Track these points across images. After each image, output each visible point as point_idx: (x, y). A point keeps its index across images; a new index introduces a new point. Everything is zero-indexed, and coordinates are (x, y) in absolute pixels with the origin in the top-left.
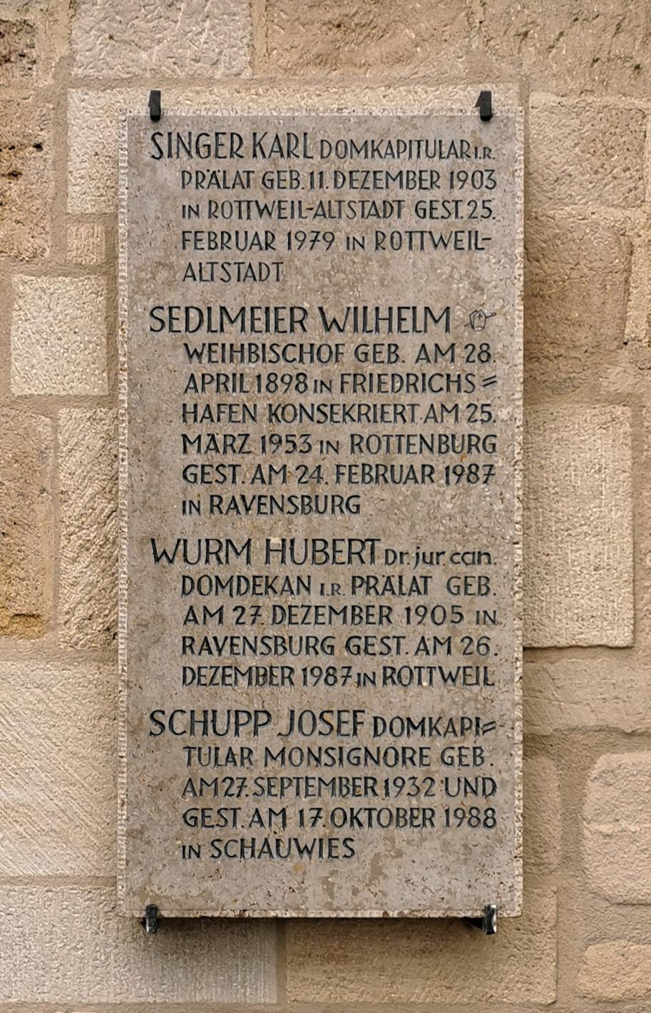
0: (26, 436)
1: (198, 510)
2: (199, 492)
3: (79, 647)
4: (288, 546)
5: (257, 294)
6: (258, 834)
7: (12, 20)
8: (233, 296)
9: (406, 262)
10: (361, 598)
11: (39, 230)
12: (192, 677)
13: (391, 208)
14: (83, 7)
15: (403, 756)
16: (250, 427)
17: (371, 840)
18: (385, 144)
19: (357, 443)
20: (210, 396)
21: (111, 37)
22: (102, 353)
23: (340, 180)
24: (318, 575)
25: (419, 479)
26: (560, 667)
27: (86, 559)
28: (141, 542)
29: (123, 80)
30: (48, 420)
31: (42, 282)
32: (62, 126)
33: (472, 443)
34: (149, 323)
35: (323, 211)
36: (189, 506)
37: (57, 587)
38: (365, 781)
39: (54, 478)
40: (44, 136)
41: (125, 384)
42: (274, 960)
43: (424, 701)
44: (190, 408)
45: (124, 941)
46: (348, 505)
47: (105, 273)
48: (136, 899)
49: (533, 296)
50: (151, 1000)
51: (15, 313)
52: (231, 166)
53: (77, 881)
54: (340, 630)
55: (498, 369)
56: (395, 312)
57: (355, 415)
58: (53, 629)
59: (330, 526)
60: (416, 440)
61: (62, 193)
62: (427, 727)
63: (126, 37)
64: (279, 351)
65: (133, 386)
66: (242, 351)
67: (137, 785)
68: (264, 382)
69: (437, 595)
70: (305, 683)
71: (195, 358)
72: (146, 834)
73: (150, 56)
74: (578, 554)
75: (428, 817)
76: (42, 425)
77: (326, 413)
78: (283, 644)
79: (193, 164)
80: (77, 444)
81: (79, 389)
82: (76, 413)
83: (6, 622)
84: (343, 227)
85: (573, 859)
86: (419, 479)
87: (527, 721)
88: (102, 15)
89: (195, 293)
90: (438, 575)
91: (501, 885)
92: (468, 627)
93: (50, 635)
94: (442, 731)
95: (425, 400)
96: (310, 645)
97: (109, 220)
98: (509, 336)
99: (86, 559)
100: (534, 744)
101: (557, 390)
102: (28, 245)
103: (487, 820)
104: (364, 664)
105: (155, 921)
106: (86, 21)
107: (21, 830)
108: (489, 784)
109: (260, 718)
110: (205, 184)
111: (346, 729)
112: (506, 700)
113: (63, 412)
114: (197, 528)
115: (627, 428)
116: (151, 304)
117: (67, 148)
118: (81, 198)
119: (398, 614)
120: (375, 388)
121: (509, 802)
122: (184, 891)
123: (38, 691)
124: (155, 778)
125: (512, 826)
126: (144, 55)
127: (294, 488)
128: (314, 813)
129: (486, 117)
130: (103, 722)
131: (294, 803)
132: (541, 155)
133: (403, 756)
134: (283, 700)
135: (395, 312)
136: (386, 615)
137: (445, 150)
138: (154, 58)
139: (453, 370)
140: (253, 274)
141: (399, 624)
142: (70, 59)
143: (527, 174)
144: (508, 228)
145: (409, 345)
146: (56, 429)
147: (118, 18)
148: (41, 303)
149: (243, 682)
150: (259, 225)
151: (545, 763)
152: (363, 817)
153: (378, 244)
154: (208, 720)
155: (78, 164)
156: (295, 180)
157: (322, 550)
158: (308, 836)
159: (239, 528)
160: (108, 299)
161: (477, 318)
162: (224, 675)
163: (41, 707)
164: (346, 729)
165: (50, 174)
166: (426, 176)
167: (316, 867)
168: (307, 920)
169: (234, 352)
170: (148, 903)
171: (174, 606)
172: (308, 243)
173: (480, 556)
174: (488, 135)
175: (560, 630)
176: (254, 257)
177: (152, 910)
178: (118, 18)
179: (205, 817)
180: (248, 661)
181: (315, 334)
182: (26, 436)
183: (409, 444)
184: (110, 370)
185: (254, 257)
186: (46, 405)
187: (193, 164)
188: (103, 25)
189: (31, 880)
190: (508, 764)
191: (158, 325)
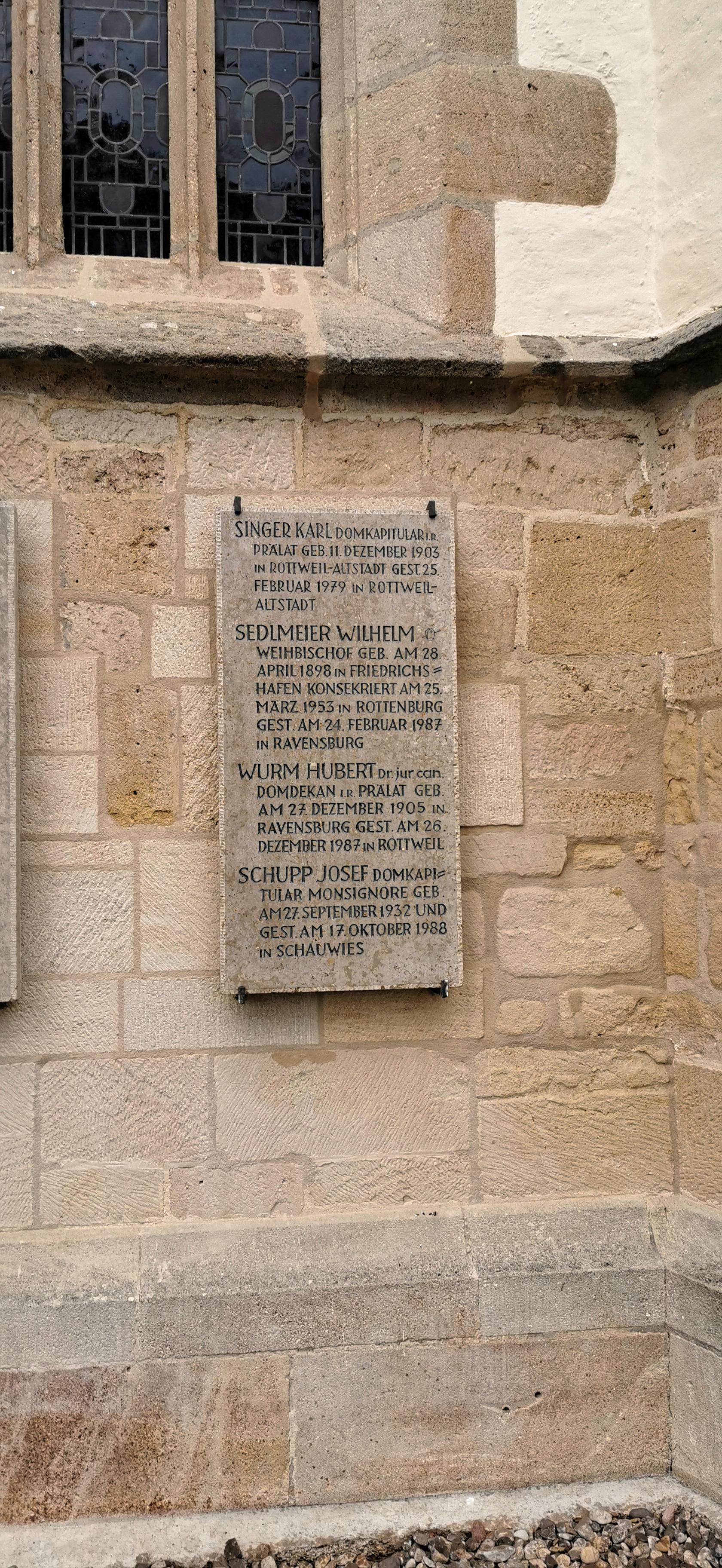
0: (161, 702)
1: (267, 746)
2: (267, 736)
3: (195, 830)
4: (321, 767)
5: (300, 618)
6: (306, 941)
7: (151, 453)
8: (286, 619)
9: (387, 599)
10: (365, 798)
11: (168, 578)
12: (263, 847)
13: (378, 568)
14: (193, 446)
15: (391, 892)
16: (297, 697)
17: (373, 943)
18: (374, 530)
19: (360, 706)
20: (273, 678)
21: (210, 465)
22: (207, 652)
23: (348, 551)
24: (339, 784)
25: (398, 727)
26: (482, 837)
27: (199, 776)
28: (233, 766)
29: (218, 490)
30: (174, 693)
31: (170, 610)
32: (181, 517)
33: (428, 706)
34: (236, 634)
35: (338, 569)
36: (261, 744)
37: (181, 793)
38: (370, 907)
39: (179, 727)
40: (170, 522)
41: (221, 671)
42: (316, 1017)
43: (403, 859)
44: (261, 686)
45: (225, 1009)
46: (356, 743)
47: (208, 605)
48: (232, 983)
49: (462, 620)
50: (242, 1045)
51: (153, 628)
52: (283, 542)
53: (195, 973)
54: (352, 818)
55: (442, 662)
56: (382, 629)
57: (359, 689)
58: (179, 819)
59: (345, 755)
60: (395, 705)
61: (181, 557)
62: (405, 875)
63: (219, 464)
64: (314, 651)
65: (226, 672)
66: (292, 652)
67: (232, 913)
68: (305, 670)
69: (410, 796)
70: (332, 850)
71: (263, 655)
72: (238, 943)
73: (234, 476)
74: (491, 771)
75: (407, 928)
76: (171, 696)
77: (342, 688)
78: (318, 827)
79: (261, 540)
80: (192, 708)
81: (194, 674)
82: (192, 688)
83: (150, 815)
84: (351, 579)
85: (491, 951)
86: (398, 727)
87: (463, 870)
88: (205, 451)
89: (263, 617)
90: (410, 784)
91: (451, 968)
92: (428, 815)
93: (176, 824)
94: (414, 877)
95: (401, 681)
96: (335, 827)
97: (211, 573)
98: (448, 643)
99: (199, 776)
100: (467, 883)
101: (477, 675)
102: (161, 587)
103: (441, 929)
104: (367, 838)
105: (244, 997)
106: (195, 454)
107: (160, 942)
108: (442, 908)
109: (305, 871)
110: (268, 552)
111: (358, 876)
112: (451, 858)
113: (184, 688)
114: (267, 757)
115: (517, 697)
116: (236, 623)
117: (184, 530)
118: (193, 559)
119: (387, 808)
120: (371, 674)
121: (454, 918)
122: (262, 977)
123: (170, 857)
124: (242, 909)
125: (456, 933)
126: (230, 476)
127: (324, 733)
128: (339, 927)
129: (433, 516)
130: (211, 875)
131: (327, 922)
132: (464, 539)
133: (391, 892)
134: (319, 860)
135: (382, 629)
136: (379, 808)
137: (409, 534)
138: (236, 477)
139: (416, 663)
140: (298, 606)
141: (387, 814)
142: (186, 476)
143: (457, 550)
144: (446, 581)
145: (390, 648)
146: (179, 698)
147: (215, 453)
148: (169, 622)
149: (295, 849)
150: (300, 577)
151: (476, 896)
152: (368, 929)
153: (371, 589)
154: (275, 873)
155: (191, 539)
156: (322, 551)
157: (341, 770)
158: (335, 942)
159: (291, 757)
160: (210, 620)
161: (430, 633)
162: (283, 846)
163: (172, 867)
164: (358, 876)
165: (174, 545)
166: (398, 550)
167: (340, 960)
168: (336, 992)
169: (287, 652)
170: (239, 985)
171: (253, 804)
172: (330, 588)
173: (434, 773)
174: (434, 526)
175: (481, 815)
176: (298, 596)
177: (242, 989)
178: (215, 453)
179: (274, 931)
180: (298, 837)
181: (335, 641)
182: (161, 702)
183: (391, 707)
184: (212, 663)
185: (298, 596)
186: (173, 684)
187: (261, 540)
188: (205, 457)
189: (167, 973)
190: (453, 896)
191: (241, 636)
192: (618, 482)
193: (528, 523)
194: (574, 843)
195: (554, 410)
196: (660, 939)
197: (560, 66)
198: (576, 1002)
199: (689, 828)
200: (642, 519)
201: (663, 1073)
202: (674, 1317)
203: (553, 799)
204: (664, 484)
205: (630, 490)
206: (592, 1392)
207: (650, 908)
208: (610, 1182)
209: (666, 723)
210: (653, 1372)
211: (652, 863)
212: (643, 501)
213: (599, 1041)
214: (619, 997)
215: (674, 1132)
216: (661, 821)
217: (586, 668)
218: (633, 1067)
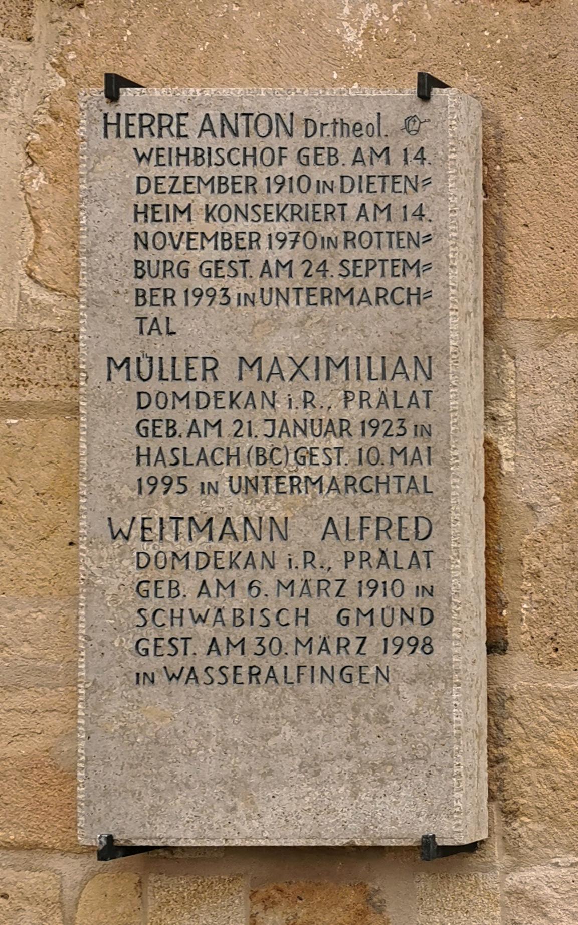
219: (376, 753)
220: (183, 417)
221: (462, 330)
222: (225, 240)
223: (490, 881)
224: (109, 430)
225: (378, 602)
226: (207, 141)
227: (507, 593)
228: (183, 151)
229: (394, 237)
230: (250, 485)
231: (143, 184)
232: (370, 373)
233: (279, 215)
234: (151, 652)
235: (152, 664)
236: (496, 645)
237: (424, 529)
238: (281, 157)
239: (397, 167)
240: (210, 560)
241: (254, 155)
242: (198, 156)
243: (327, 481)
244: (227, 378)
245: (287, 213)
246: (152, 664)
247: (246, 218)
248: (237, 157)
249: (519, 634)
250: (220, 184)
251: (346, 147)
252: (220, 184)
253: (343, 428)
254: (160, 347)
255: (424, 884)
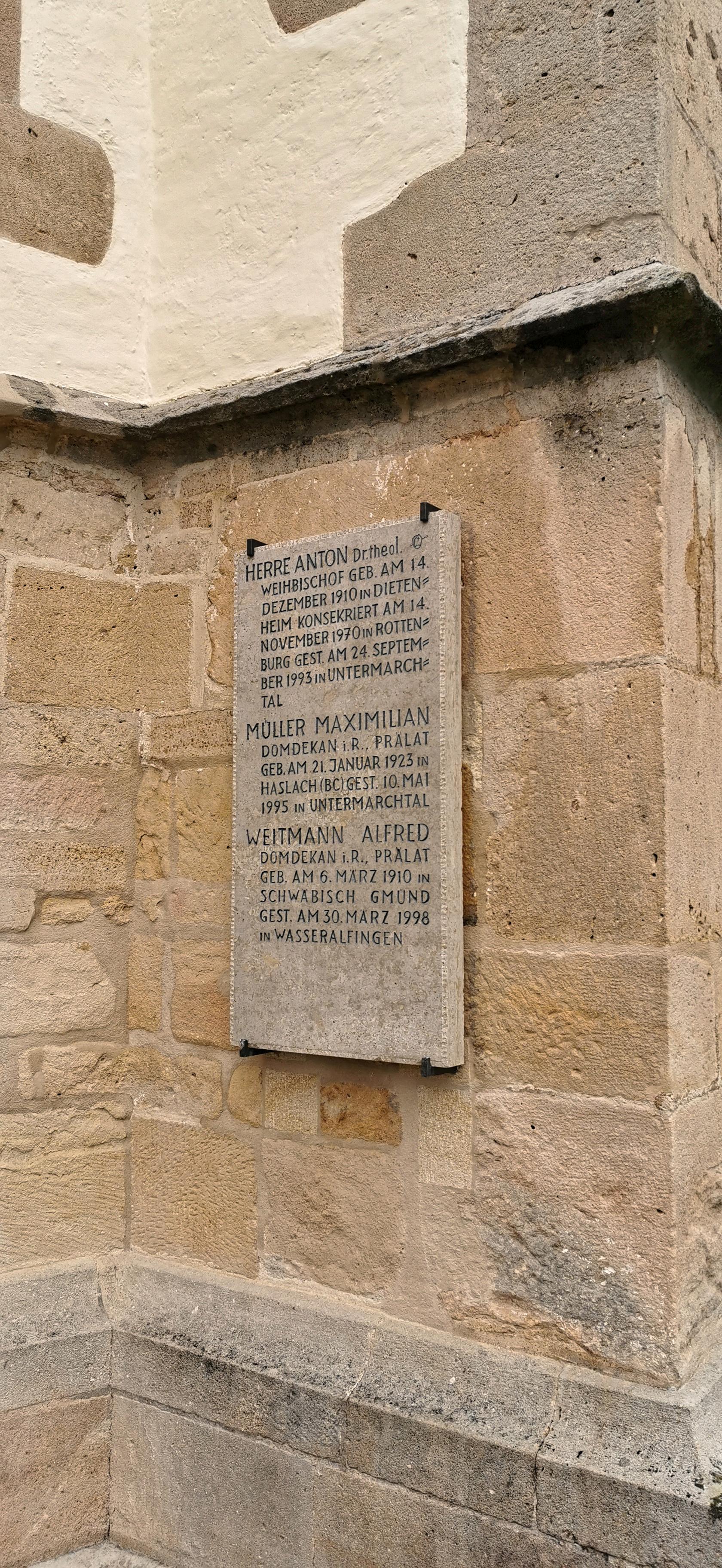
192: (104, 538)
193: (11, 567)
194: (43, 897)
195: (42, 458)
196: (124, 994)
197: (62, 119)
198: (36, 1062)
199: (159, 883)
200: (126, 578)
201: (120, 1129)
202: (119, 1378)
203: (24, 851)
204: (148, 547)
205: (116, 548)
206: (29, 1472)
207: (116, 963)
208: (61, 1247)
209: (141, 779)
210: (96, 1437)
211: (120, 918)
212: (128, 560)
213: (57, 1101)
214: (80, 1054)
215: (128, 1187)
216: (131, 875)
217: (64, 719)
218: (93, 1125)
219: (394, 995)
220: (286, 760)
221: (448, 686)
222: (310, 639)
223: (465, 1097)
224: (248, 771)
225: (395, 886)
226: (301, 574)
227: (477, 880)
228: (287, 583)
229: (406, 623)
230: (321, 805)
231: (267, 608)
232: (391, 722)
233: (339, 617)
234: (268, 919)
235: (269, 927)
236: (469, 920)
237: (424, 833)
238: (340, 577)
239: (408, 574)
240: (299, 857)
241: (325, 579)
242: (295, 585)
243: (365, 800)
244: (310, 734)
245: (343, 616)
246: (269, 927)
247: (320, 622)
248: (316, 582)
249: (485, 911)
250: (307, 602)
251: (377, 564)
252: (307, 602)
253: (373, 763)
254: (275, 715)
255: (423, 1094)
